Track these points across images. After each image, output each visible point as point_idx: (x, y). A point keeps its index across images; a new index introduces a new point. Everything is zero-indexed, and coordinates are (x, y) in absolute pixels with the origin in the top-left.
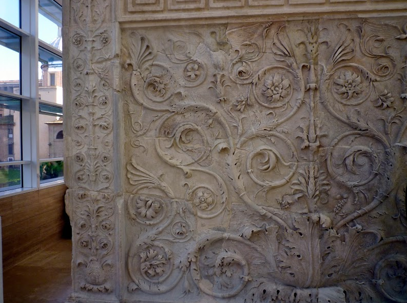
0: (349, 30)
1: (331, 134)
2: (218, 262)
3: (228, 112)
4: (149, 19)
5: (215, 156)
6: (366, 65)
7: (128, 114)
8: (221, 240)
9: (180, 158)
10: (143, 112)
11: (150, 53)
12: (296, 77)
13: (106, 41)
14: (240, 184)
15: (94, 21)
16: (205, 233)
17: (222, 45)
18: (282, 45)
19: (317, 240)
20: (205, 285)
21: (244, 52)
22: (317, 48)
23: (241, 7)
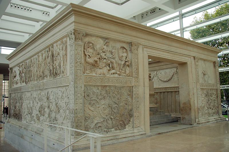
1: (112, 104)
2: (98, 127)
3: (99, 100)
5: (97, 108)
6: (116, 93)
8: (98, 123)
10: (86, 100)
12: (108, 95)
15: (80, 84)
16: (96, 122)
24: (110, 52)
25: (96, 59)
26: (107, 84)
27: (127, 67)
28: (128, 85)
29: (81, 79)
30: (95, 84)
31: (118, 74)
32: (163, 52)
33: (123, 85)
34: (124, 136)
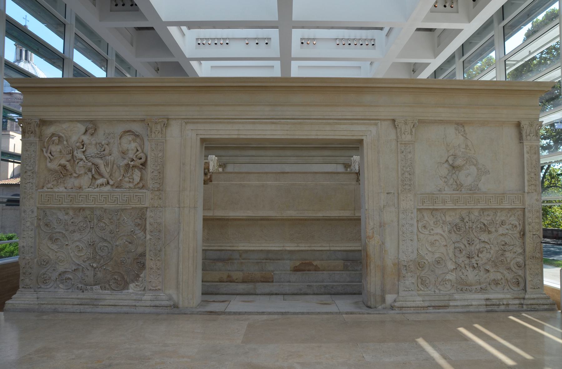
5: (65, 246)
6: (107, 221)
7: (39, 234)
8: (66, 272)
9: (54, 247)
13: (33, 212)
14: (72, 255)
16: (61, 269)
17: (67, 214)
19: (93, 272)
20: (61, 286)
24: (98, 146)
25: (63, 162)
26: (84, 206)
27: (136, 170)
28: (134, 206)
29: (32, 198)
30: (59, 206)
31: (112, 185)
32: (254, 123)
34: (112, 302)
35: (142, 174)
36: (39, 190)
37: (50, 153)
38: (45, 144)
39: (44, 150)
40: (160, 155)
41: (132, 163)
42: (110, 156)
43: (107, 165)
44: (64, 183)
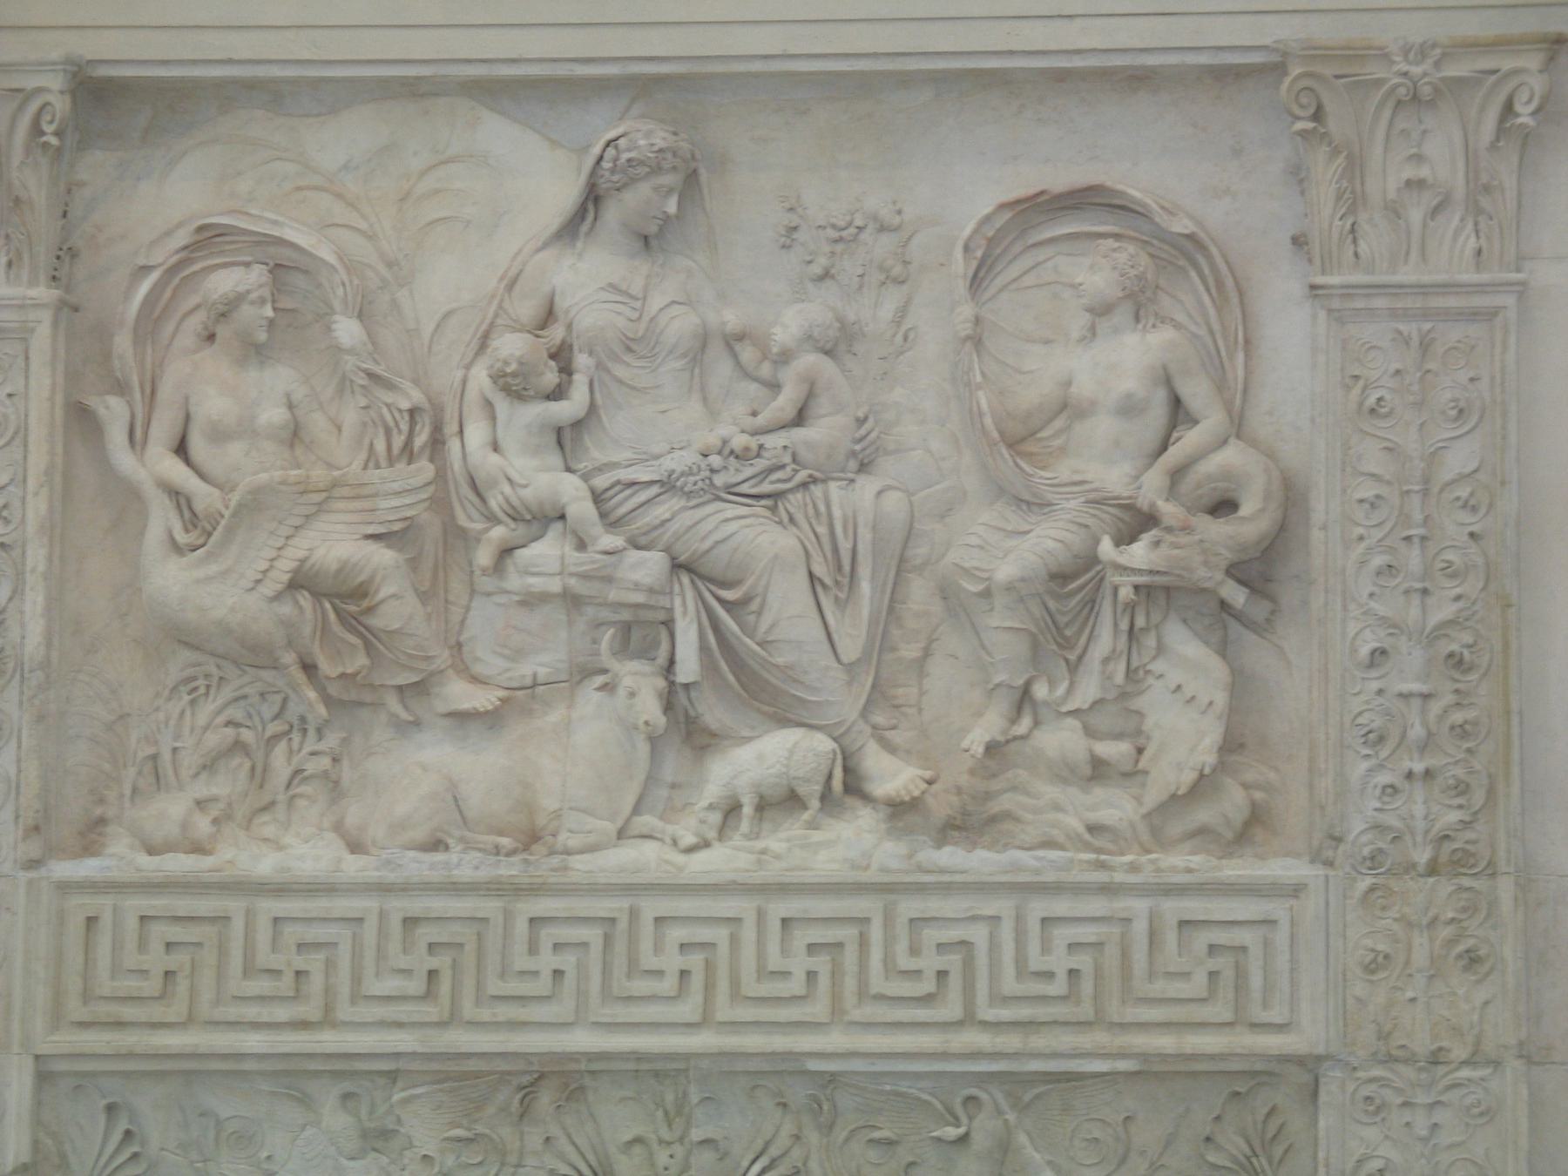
0: (785, 1105)
4: (138, 1050)
11: (135, 1156)
18: (574, 1144)
21: (450, 1161)
22: (687, 1158)
23: (441, 1025)
24: (722, 369)
25: (336, 544)
26: (582, 1040)
28: (1165, 1042)
31: (900, 810)
33: (1011, 1041)
35: (1241, 684)
36: (64, 869)
37: (181, 449)
38: (123, 343)
39: (114, 412)
40: (1459, 460)
41: (1139, 553)
42: (867, 487)
43: (831, 580)
44: (335, 788)
